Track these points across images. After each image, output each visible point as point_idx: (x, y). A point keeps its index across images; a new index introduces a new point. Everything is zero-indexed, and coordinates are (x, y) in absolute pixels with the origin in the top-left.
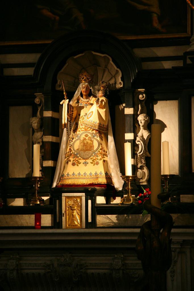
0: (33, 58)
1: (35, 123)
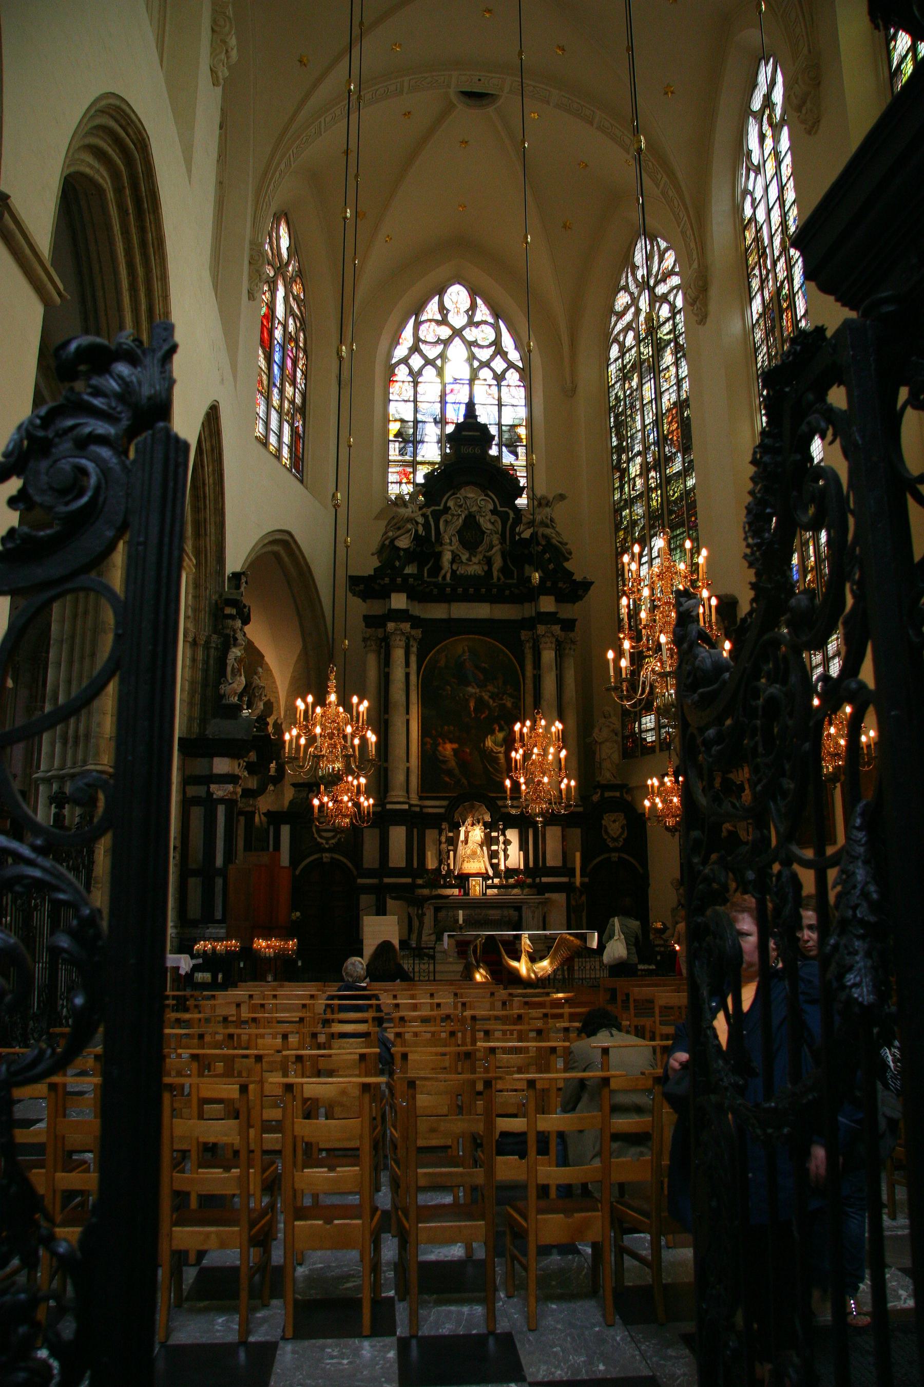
0: (445, 803)
1: (443, 839)
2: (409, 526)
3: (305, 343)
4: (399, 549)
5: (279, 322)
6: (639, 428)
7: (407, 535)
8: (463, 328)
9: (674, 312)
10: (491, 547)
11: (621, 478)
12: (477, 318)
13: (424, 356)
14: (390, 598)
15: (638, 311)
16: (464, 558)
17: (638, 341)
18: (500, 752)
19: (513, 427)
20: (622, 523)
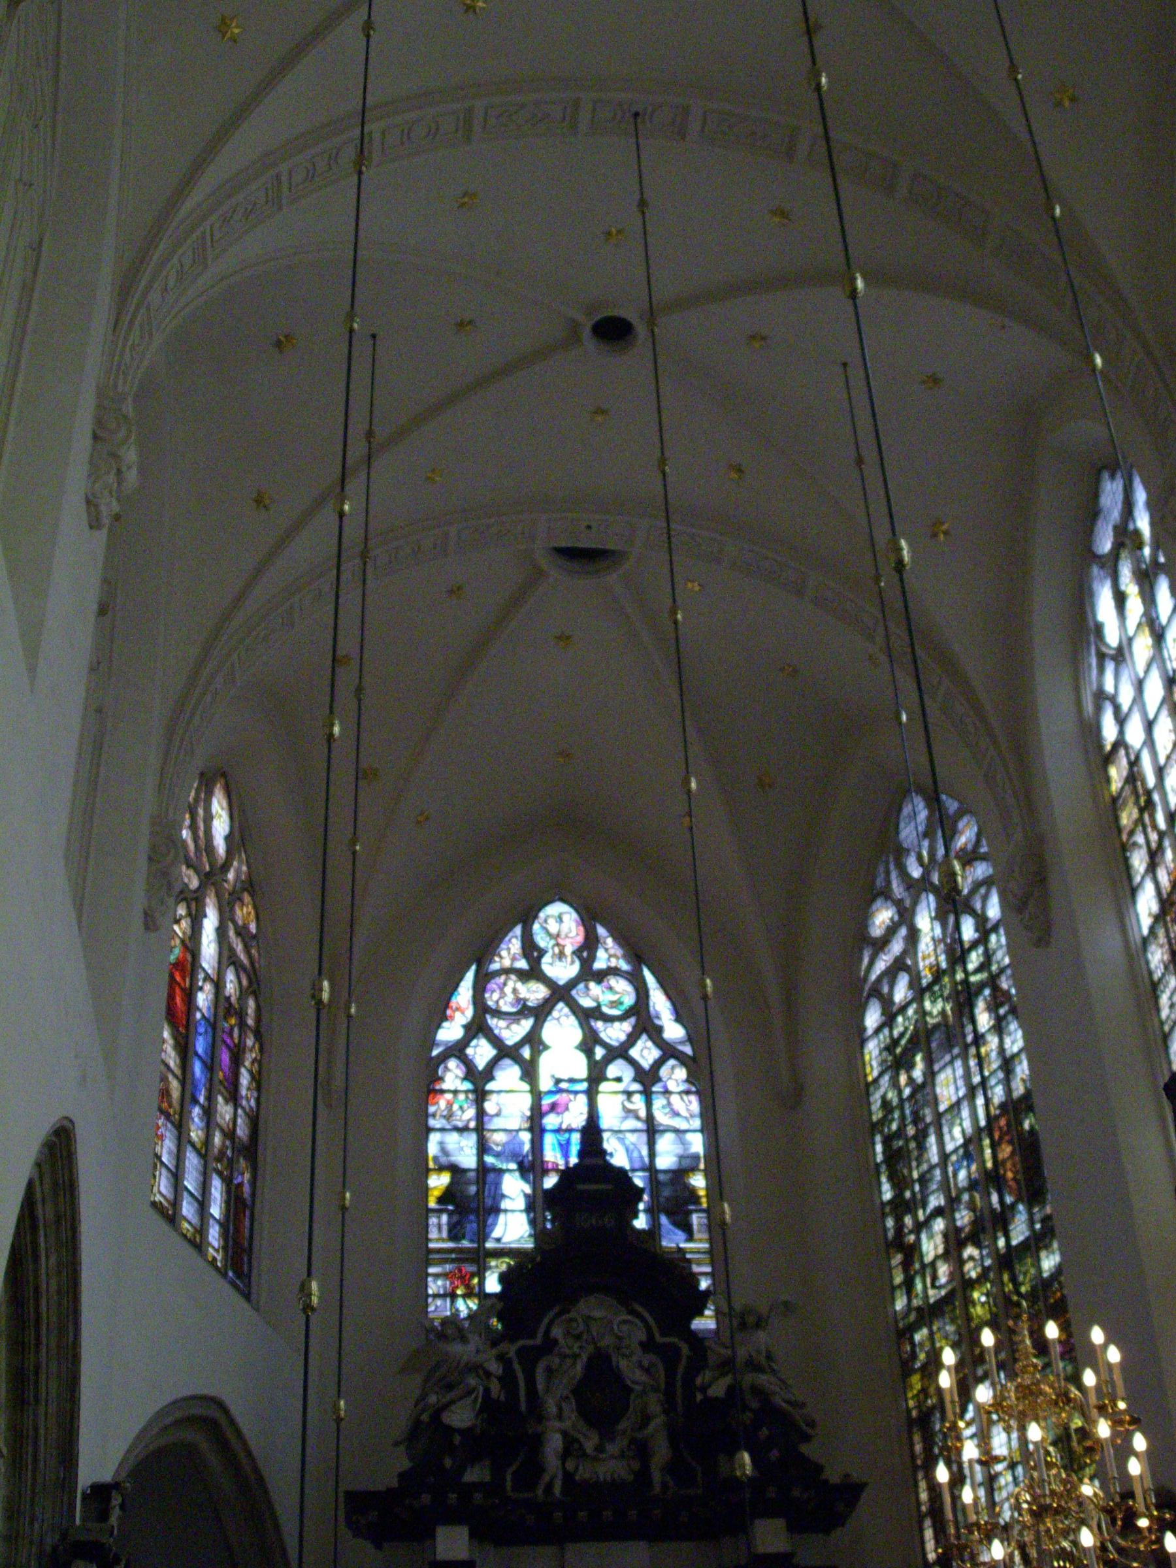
2: (472, 1381)
3: (258, 1020)
4: (449, 1430)
5: (207, 978)
6: (935, 1159)
7: (469, 1400)
8: (573, 983)
9: (984, 929)
10: (646, 1419)
11: (906, 1265)
12: (600, 964)
13: (496, 1041)
14: (433, 1536)
15: (913, 936)
16: (589, 1446)
17: (919, 992)
19: (679, 1174)
20: (914, 1356)
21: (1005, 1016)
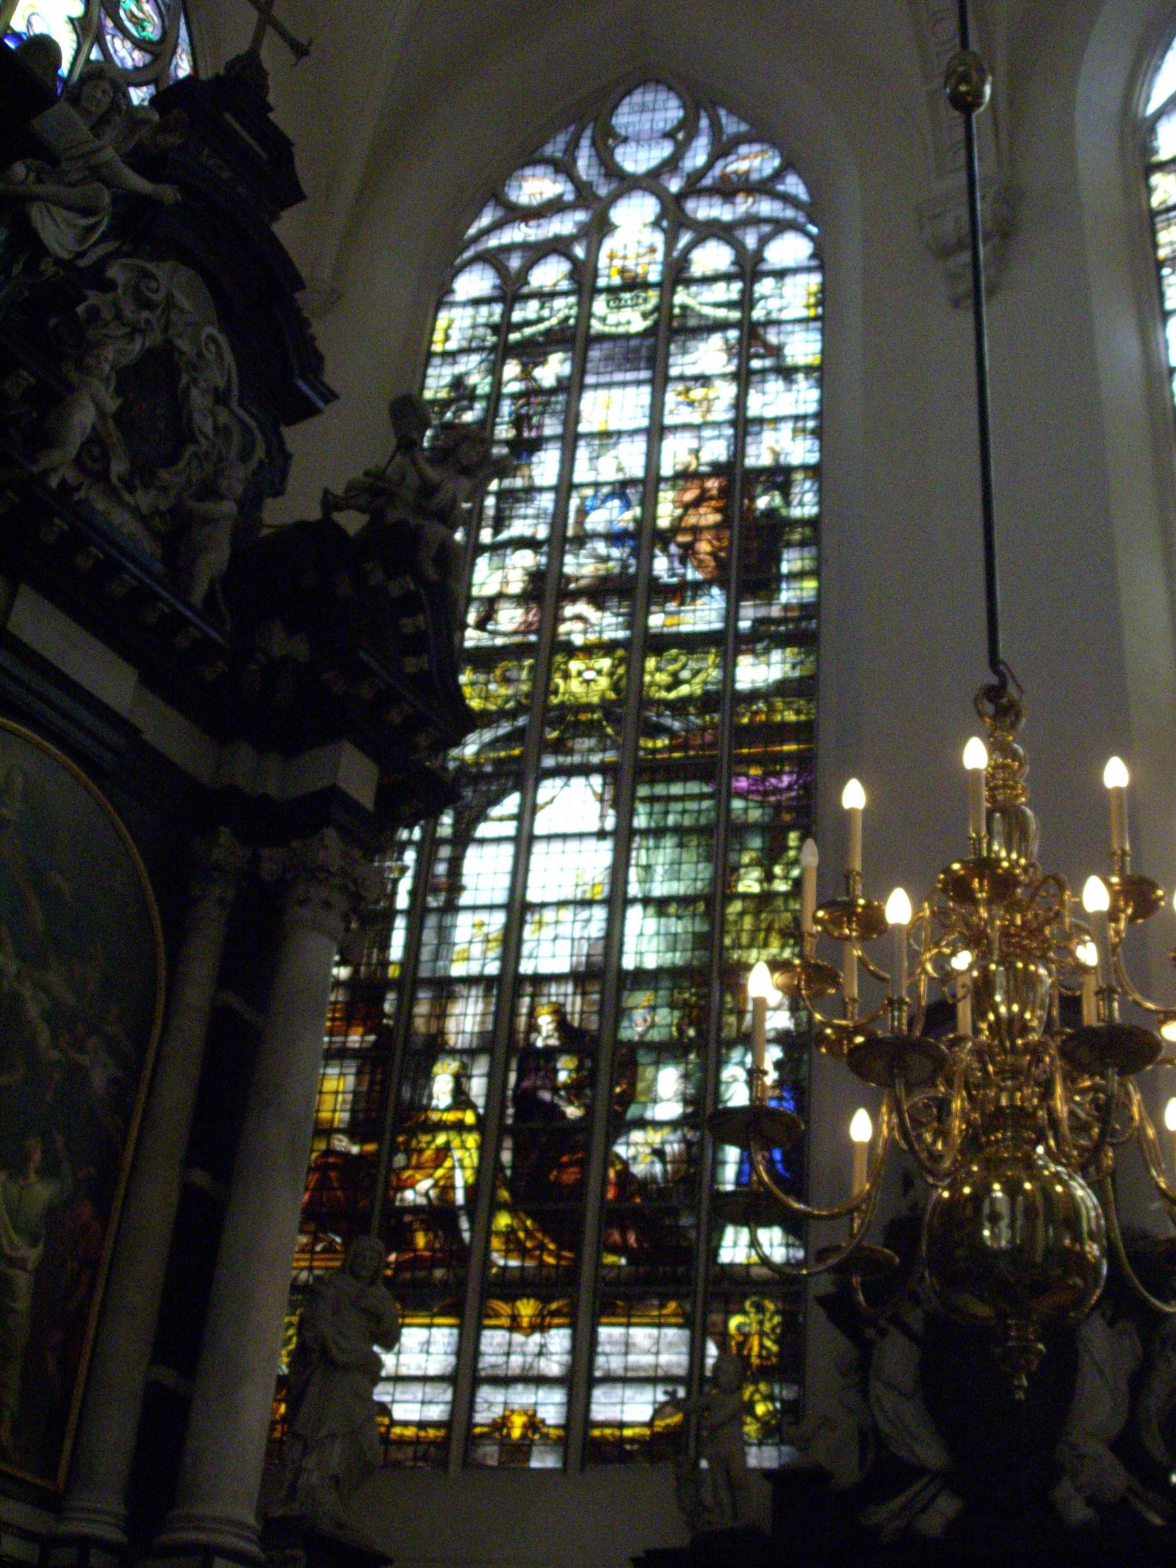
18: (20, 1264)
21: (763, 371)
